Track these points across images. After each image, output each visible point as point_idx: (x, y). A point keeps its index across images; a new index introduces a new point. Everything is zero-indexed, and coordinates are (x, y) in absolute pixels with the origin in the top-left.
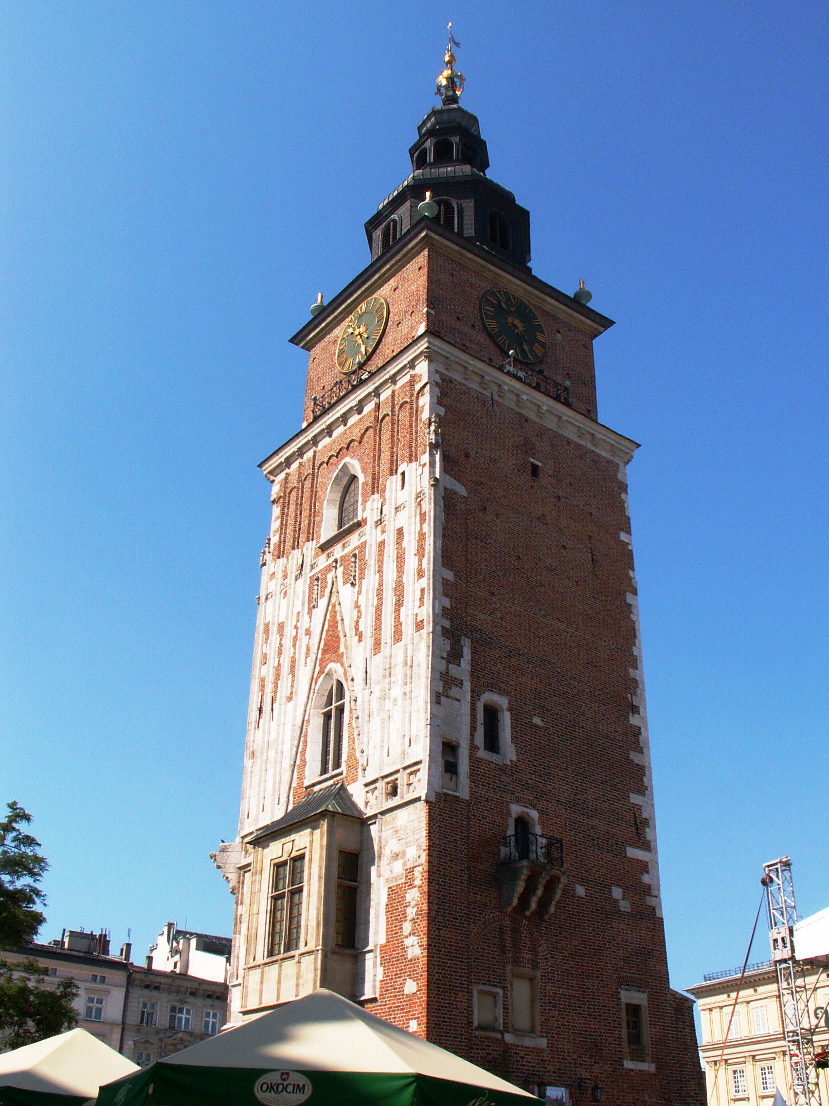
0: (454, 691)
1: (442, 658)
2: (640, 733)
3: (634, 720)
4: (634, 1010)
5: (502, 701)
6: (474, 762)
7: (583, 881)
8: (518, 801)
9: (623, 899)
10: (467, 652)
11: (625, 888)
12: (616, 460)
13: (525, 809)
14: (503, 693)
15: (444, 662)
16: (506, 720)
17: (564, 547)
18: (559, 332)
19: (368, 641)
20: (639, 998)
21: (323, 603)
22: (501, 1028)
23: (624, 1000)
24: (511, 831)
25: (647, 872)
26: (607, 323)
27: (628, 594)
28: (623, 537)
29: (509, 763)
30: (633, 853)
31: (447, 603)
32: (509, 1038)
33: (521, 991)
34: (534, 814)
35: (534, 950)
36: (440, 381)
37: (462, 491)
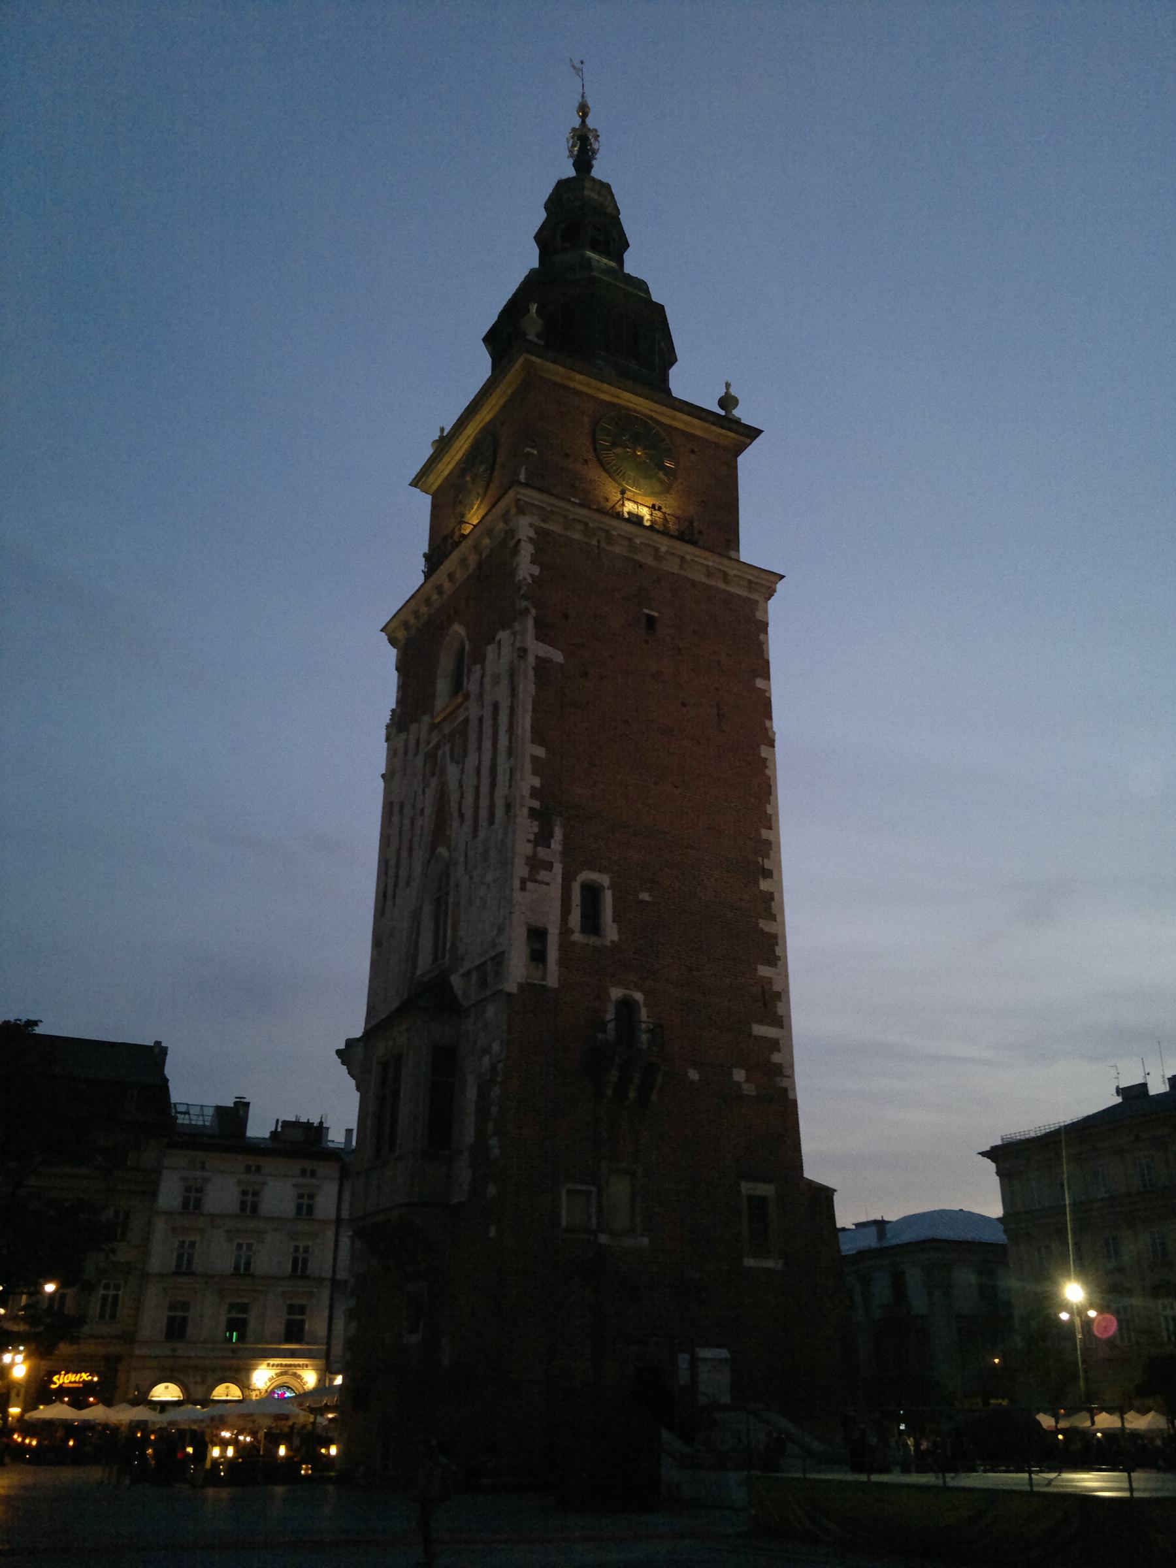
0: (543, 875)
1: (529, 841)
2: (772, 899)
3: (764, 885)
4: (758, 1204)
5: (604, 879)
6: (566, 946)
9: (747, 1081)
10: (558, 833)
12: (755, 596)
13: (627, 992)
15: (531, 845)
16: (608, 898)
17: (684, 704)
18: (693, 452)
19: (468, 822)
20: (766, 1190)
21: (434, 782)
22: (594, 1227)
23: (743, 1191)
24: (610, 1015)
25: (779, 1051)
26: (753, 433)
27: (763, 747)
28: (759, 683)
29: (608, 944)
30: (760, 1030)
31: (537, 782)
32: (603, 1239)
33: (619, 1189)
34: (639, 996)
36: (532, 533)
37: (558, 657)
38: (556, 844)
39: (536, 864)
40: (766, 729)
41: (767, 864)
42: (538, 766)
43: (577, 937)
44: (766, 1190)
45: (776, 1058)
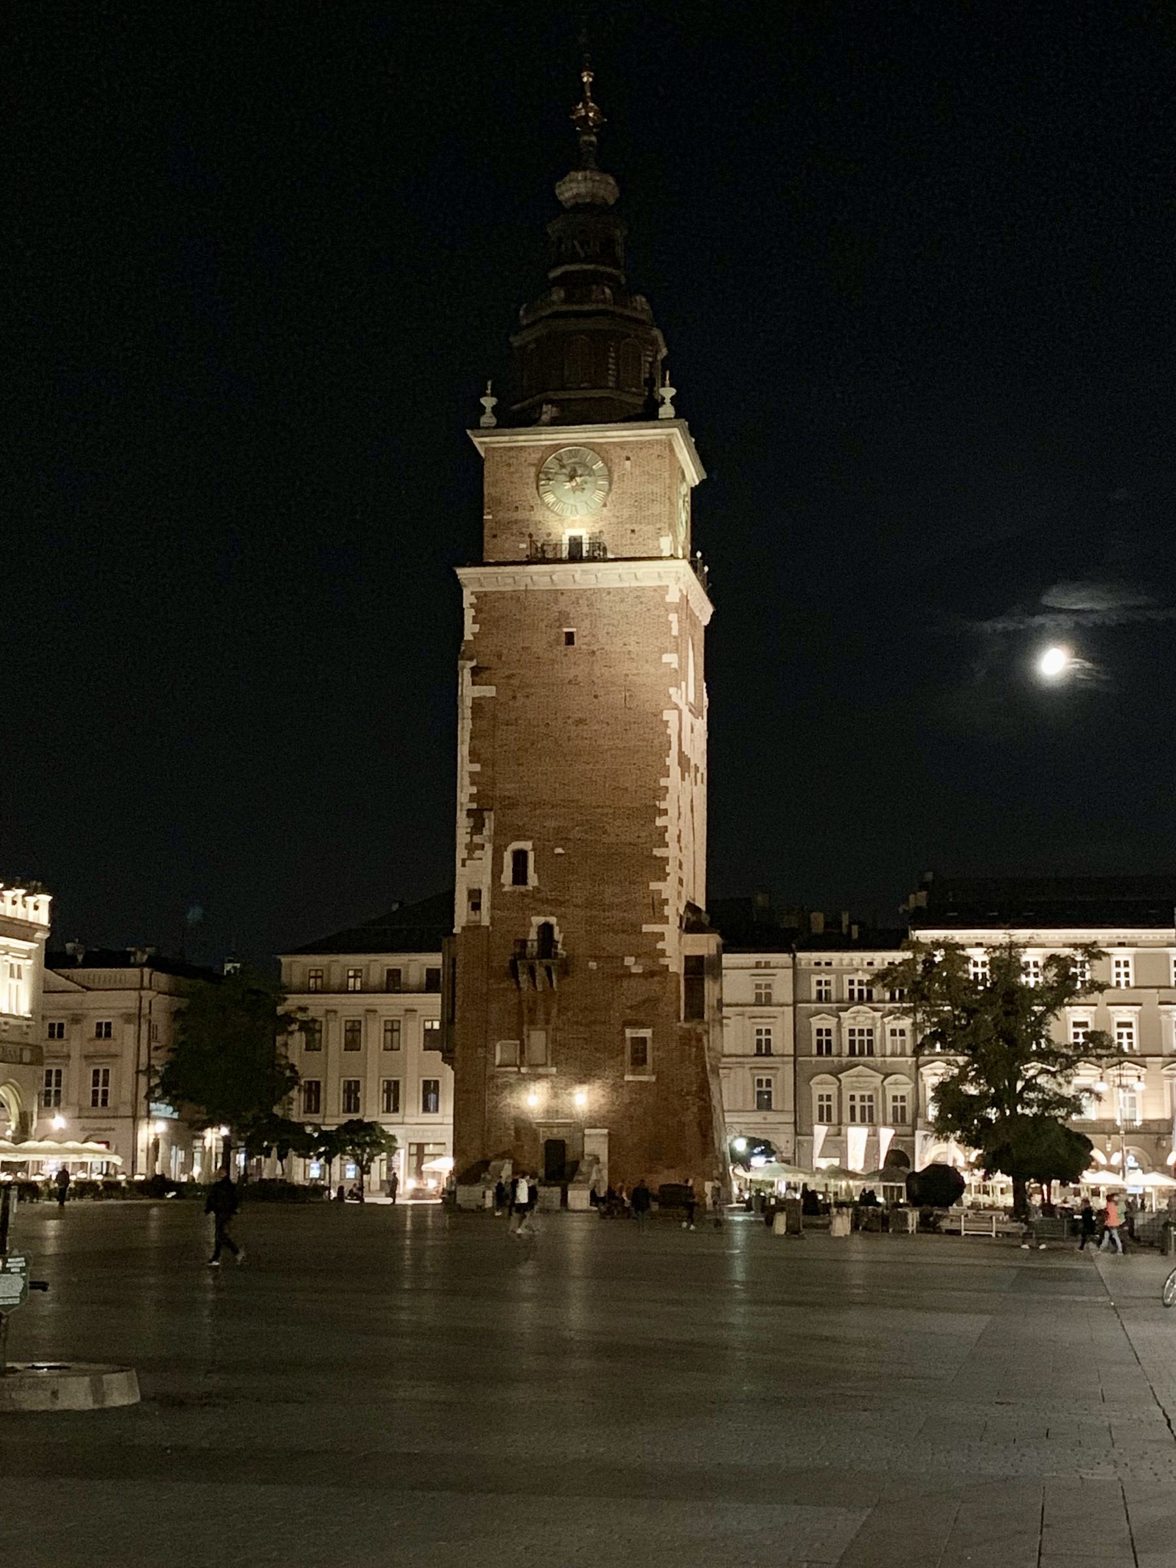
0: (478, 853)
3: (659, 822)
5: (527, 845)
7: (596, 958)
8: (538, 914)
11: (638, 956)
14: (530, 838)
16: (531, 856)
17: (596, 697)
18: (628, 459)
20: (646, 1033)
24: (533, 935)
30: (646, 928)
31: (474, 790)
34: (553, 920)
35: (548, 1013)
38: (486, 832)
39: (472, 848)
40: (670, 697)
41: (663, 805)
42: (474, 778)
43: (506, 889)
44: (646, 1033)
45: (660, 945)
